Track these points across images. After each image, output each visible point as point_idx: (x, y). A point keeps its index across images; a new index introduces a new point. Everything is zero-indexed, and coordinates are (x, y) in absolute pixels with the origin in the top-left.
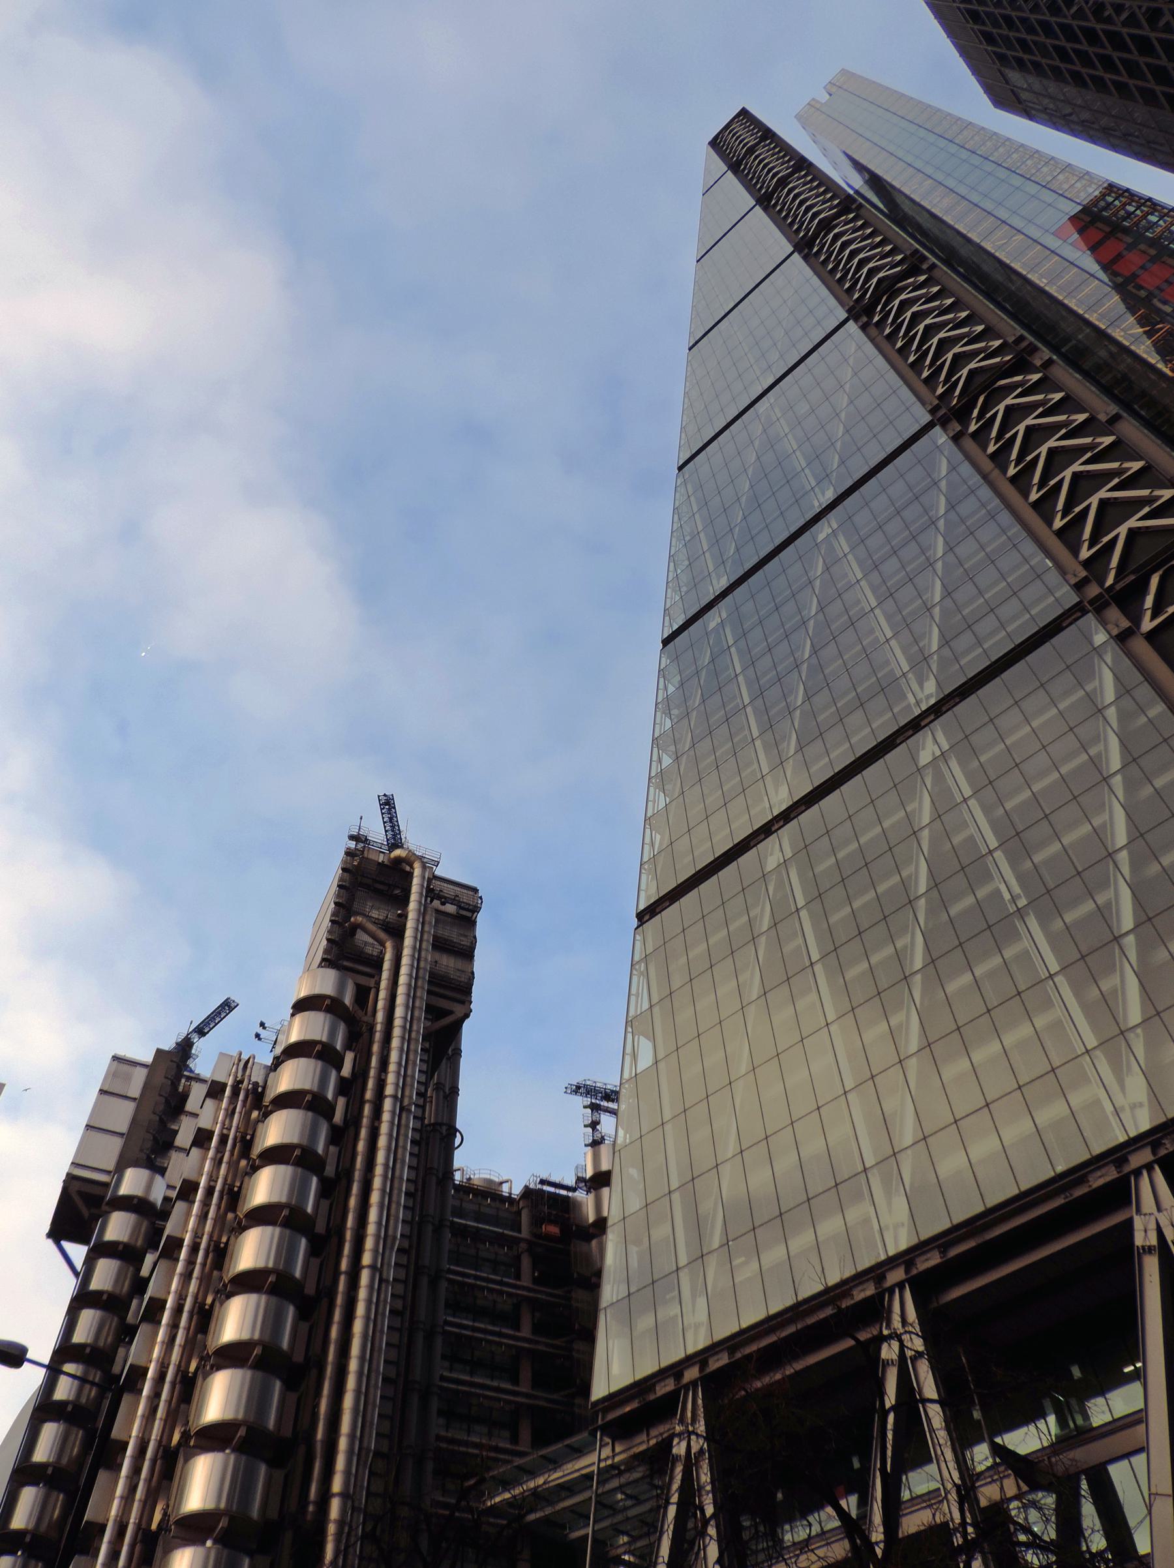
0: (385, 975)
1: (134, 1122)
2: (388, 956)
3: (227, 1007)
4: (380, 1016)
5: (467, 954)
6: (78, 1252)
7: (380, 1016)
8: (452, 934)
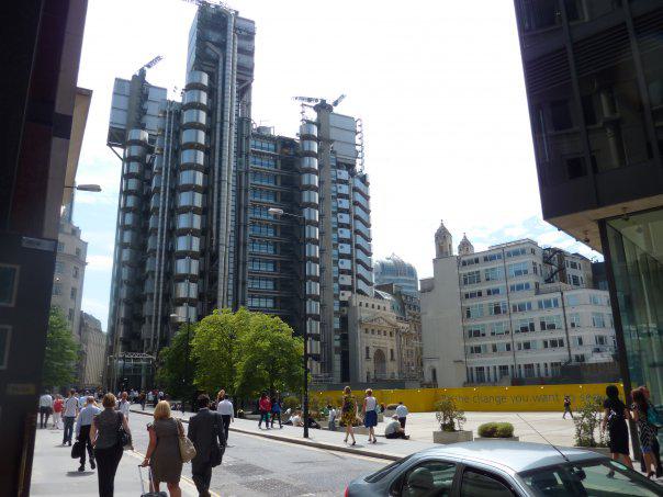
0: (221, 69)
1: (130, 105)
2: (221, 60)
3: (158, 58)
4: (220, 88)
5: (251, 53)
6: (120, 151)
7: (220, 88)
8: (245, 43)
